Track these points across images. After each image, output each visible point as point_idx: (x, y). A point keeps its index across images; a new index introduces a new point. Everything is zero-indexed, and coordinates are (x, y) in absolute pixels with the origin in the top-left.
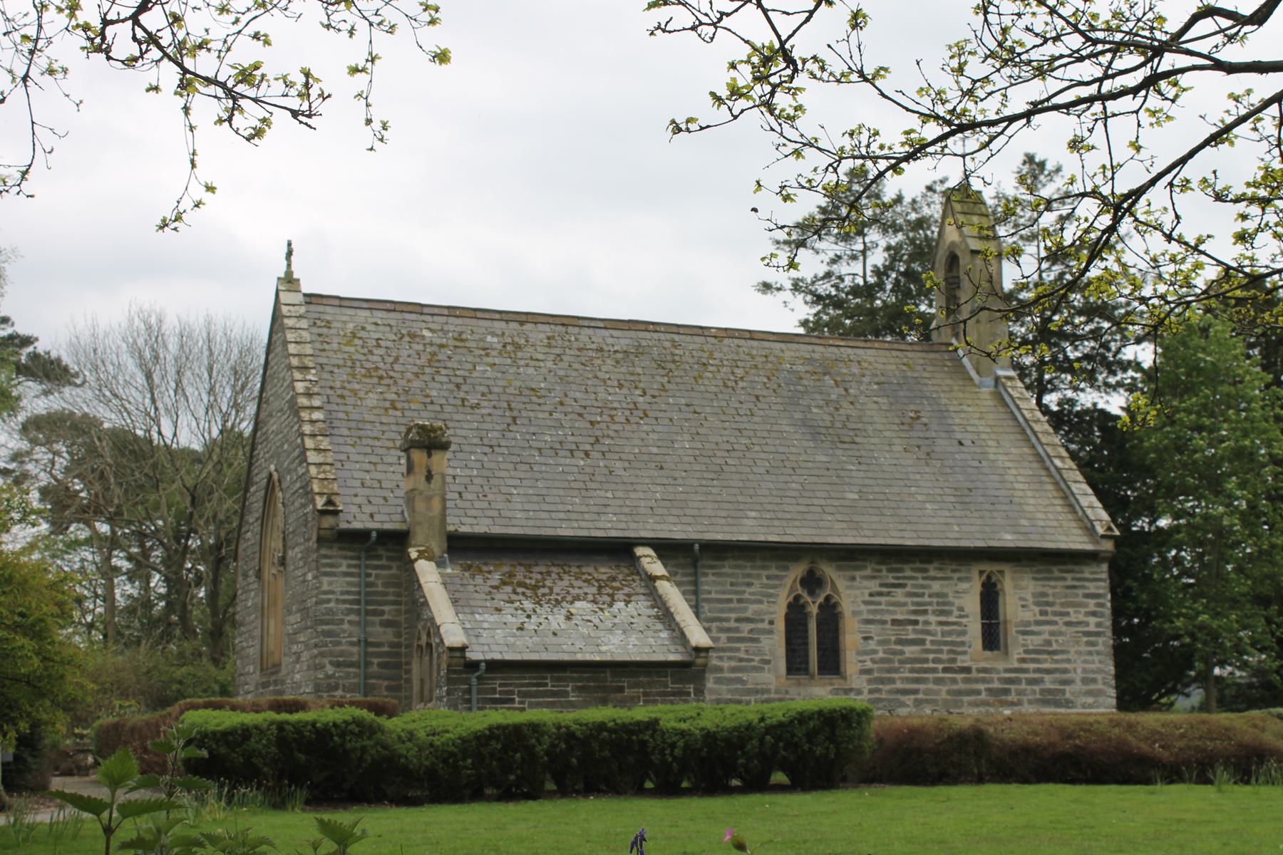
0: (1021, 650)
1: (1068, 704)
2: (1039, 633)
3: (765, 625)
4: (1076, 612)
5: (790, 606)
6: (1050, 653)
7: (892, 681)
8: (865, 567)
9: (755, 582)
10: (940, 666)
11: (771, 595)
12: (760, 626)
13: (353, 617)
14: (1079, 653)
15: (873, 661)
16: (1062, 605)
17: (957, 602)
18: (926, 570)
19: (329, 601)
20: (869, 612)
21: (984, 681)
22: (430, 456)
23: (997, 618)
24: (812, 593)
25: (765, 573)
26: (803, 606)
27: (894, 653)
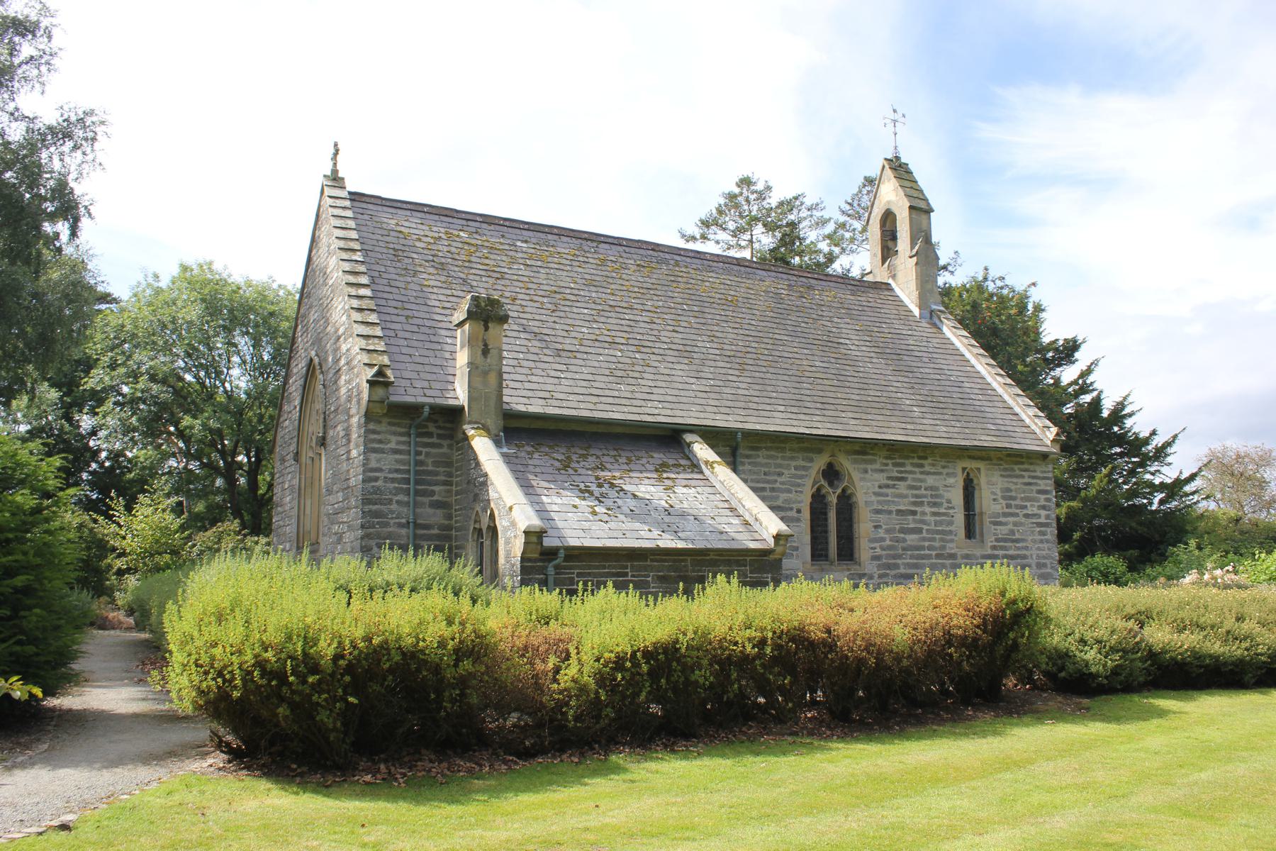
0: (993, 539)
3: (793, 514)
4: (1032, 506)
5: (813, 496)
7: (896, 566)
8: (875, 461)
9: (786, 472)
10: (934, 553)
11: (799, 485)
12: (789, 514)
13: (401, 497)
14: (1034, 541)
15: (882, 548)
16: (1022, 499)
17: (945, 494)
18: (922, 466)
19: (376, 479)
22: (487, 329)
23: (973, 511)
24: (831, 484)
25: (794, 463)
26: (824, 497)
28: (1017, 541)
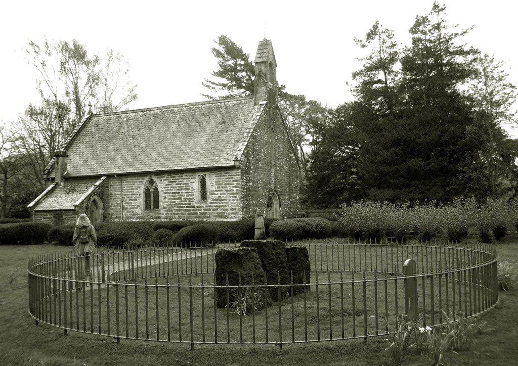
1: (226, 217)
2: (217, 194)
6: (220, 200)
7: (172, 211)
20: (166, 190)
21: (199, 210)
27: (173, 202)
28: (222, 200)
